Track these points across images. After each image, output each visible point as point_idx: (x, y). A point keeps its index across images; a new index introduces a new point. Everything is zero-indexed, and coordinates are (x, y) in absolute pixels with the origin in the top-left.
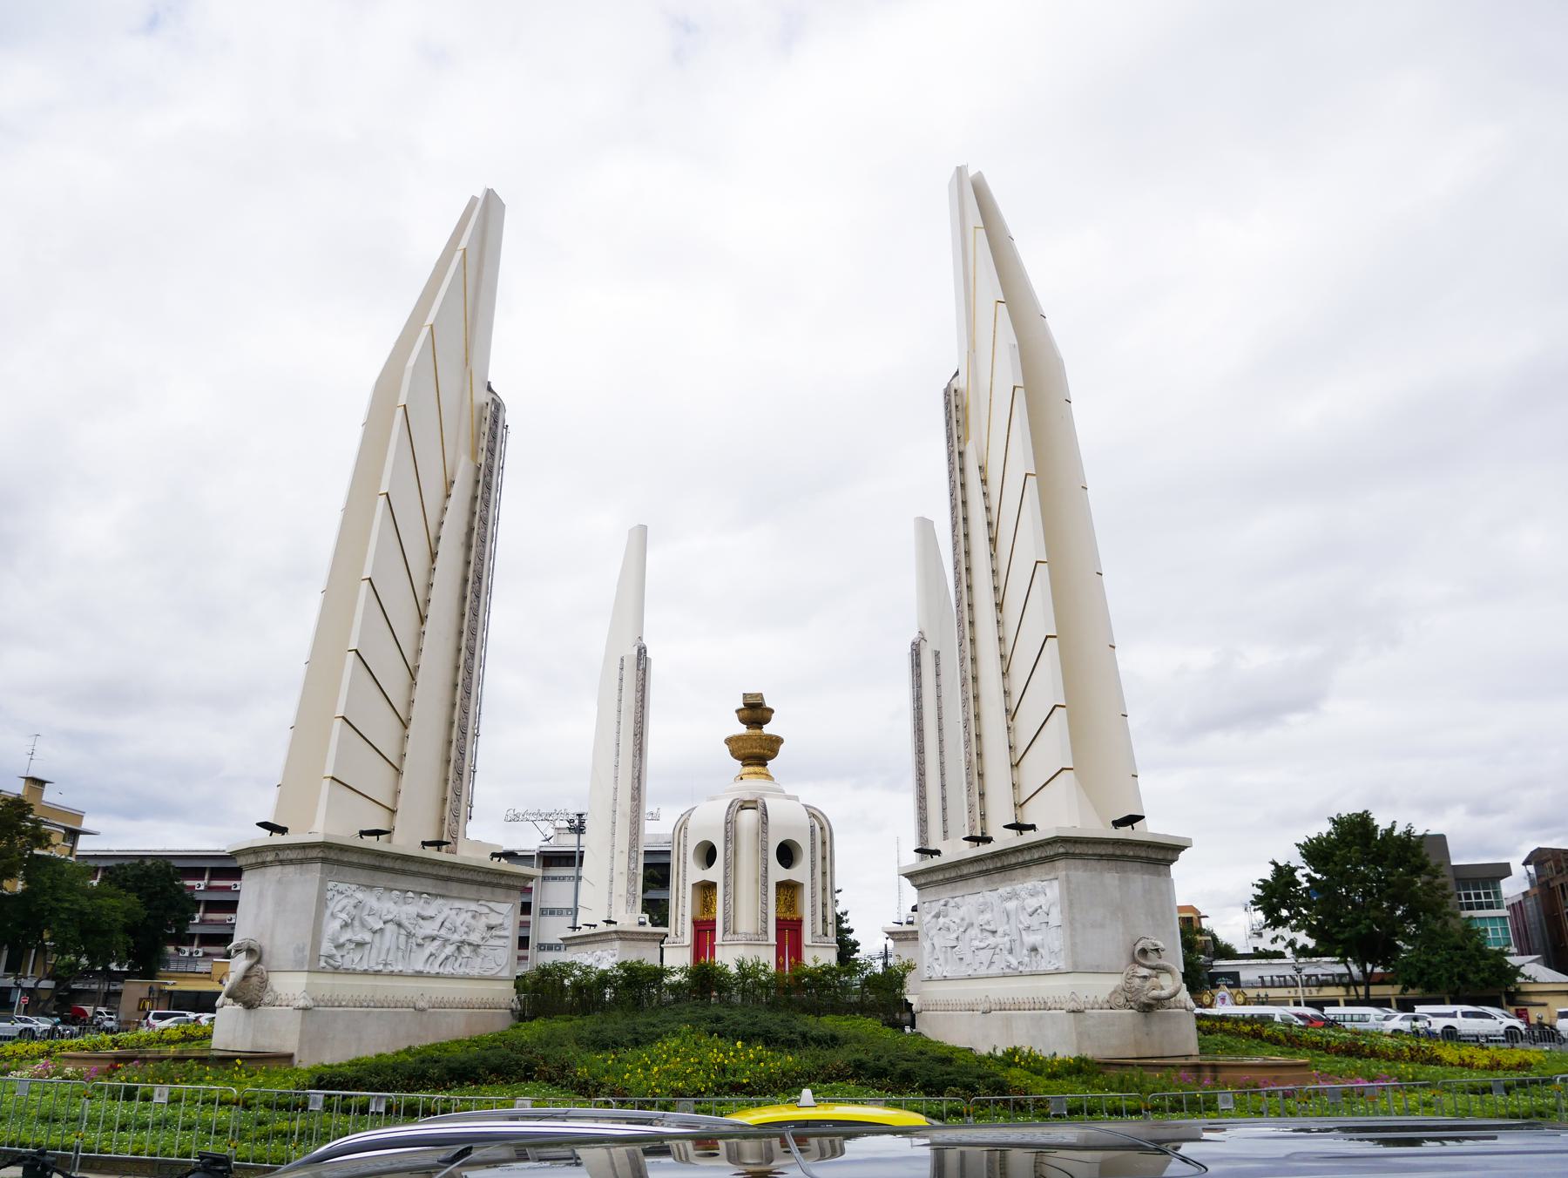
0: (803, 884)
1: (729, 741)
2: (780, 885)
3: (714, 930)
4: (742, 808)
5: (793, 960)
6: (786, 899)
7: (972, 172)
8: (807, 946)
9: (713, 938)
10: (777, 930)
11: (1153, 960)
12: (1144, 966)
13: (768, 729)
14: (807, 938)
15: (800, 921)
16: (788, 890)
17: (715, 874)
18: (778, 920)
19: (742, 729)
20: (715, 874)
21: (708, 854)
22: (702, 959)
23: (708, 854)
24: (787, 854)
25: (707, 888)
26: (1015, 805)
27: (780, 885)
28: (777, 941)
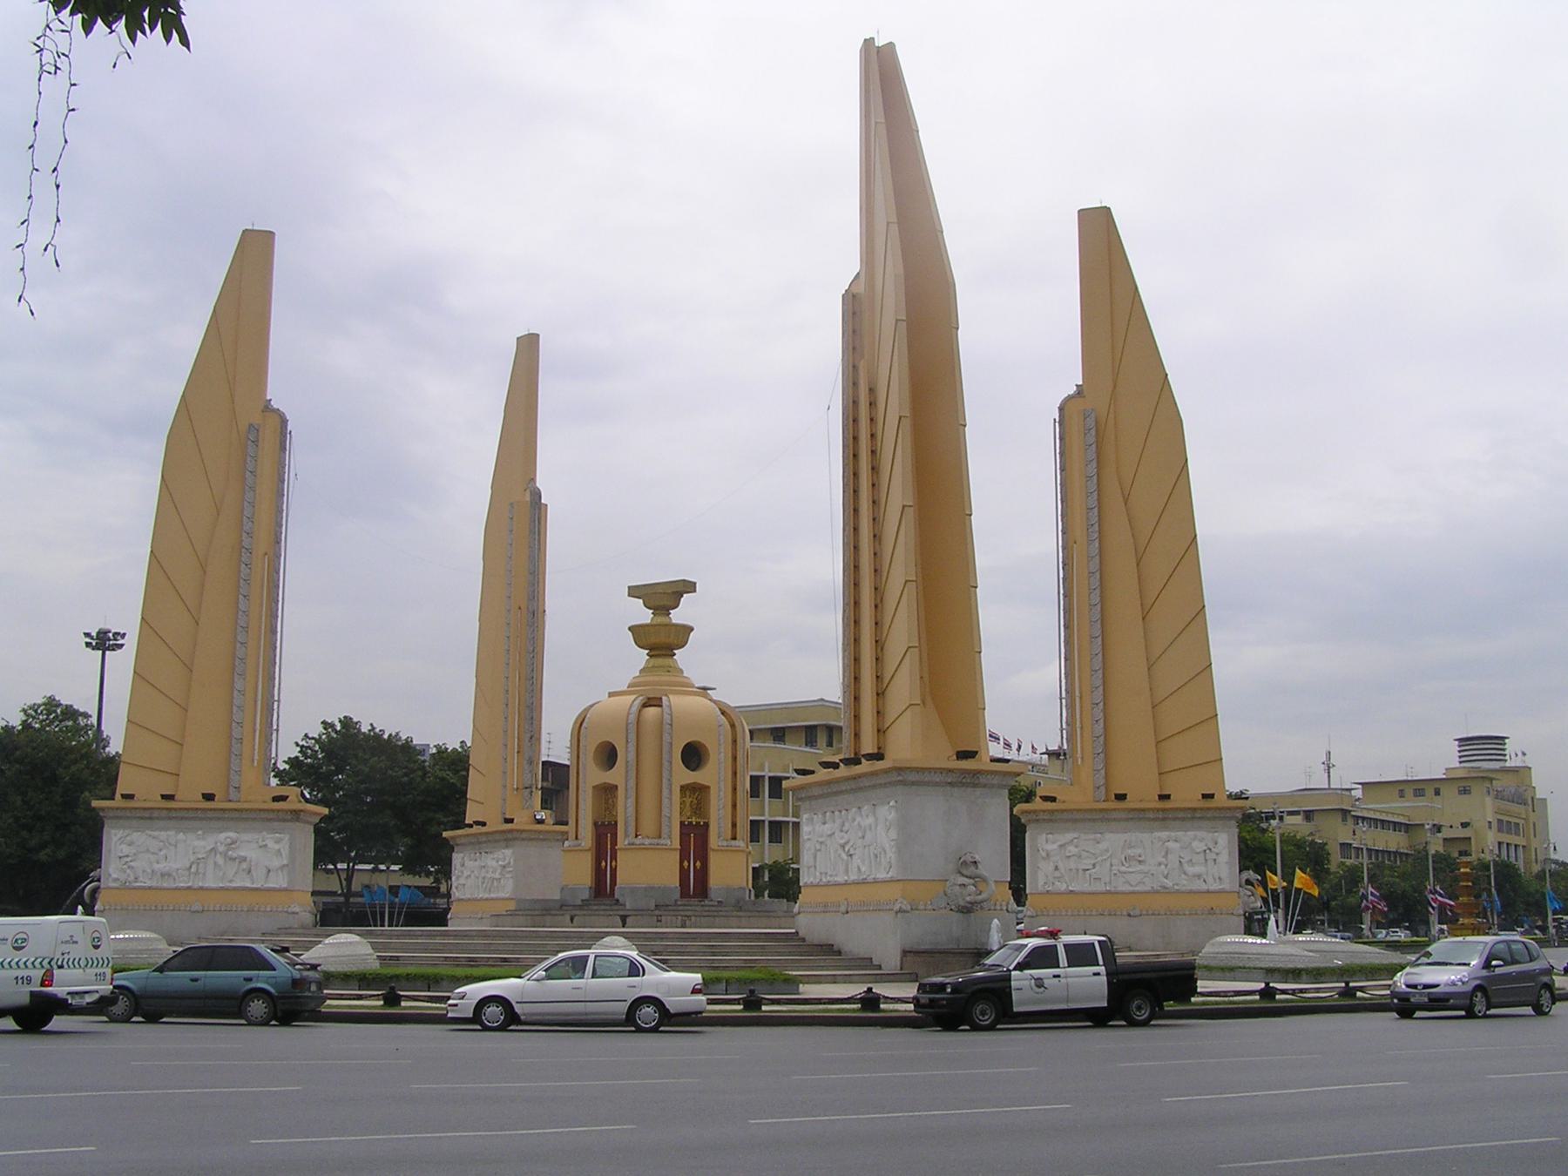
0: (708, 787)
1: (630, 629)
2: (683, 788)
3: (615, 835)
4: (645, 705)
5: (698, 864)
6: (692, 802)
7: (879, 42)
8: (713, 850)
9: (614, 843)
10: (681, 834)
11: (971, 870)
12: (963, 875)
13: (677, 616)
14: (714, 841)
15: (707, 825)
16: (696, 793)
17: (615, 776)
18: (682, 823)
19: (645, 616)
20: (615, 776)
21: (609, 755)
22: (603, 864)
23: (609, 755)
24: (693, 755)
25: (607, 792)
26: (879, 731)
27: (683, 788)
28: (681, 845)
